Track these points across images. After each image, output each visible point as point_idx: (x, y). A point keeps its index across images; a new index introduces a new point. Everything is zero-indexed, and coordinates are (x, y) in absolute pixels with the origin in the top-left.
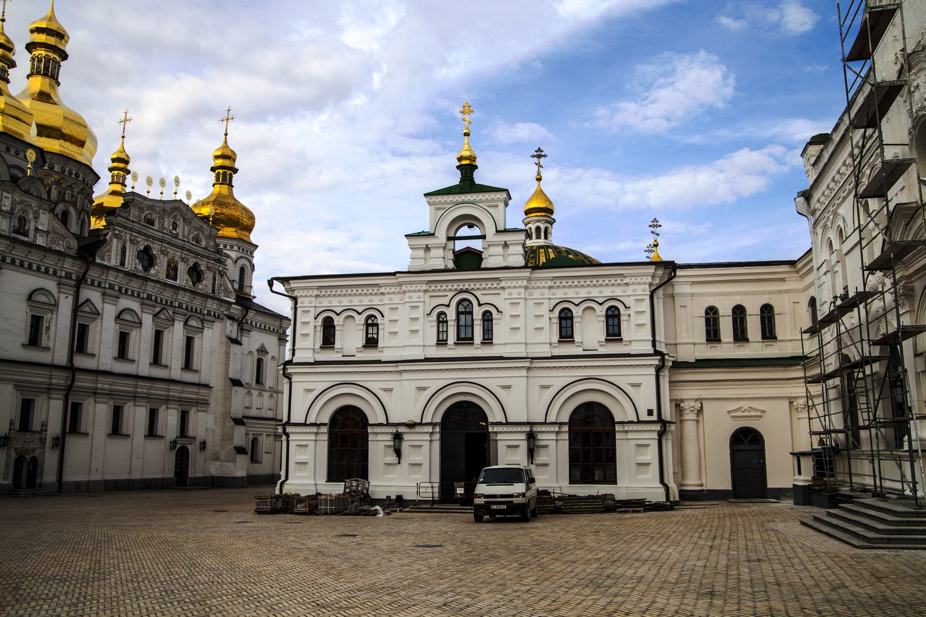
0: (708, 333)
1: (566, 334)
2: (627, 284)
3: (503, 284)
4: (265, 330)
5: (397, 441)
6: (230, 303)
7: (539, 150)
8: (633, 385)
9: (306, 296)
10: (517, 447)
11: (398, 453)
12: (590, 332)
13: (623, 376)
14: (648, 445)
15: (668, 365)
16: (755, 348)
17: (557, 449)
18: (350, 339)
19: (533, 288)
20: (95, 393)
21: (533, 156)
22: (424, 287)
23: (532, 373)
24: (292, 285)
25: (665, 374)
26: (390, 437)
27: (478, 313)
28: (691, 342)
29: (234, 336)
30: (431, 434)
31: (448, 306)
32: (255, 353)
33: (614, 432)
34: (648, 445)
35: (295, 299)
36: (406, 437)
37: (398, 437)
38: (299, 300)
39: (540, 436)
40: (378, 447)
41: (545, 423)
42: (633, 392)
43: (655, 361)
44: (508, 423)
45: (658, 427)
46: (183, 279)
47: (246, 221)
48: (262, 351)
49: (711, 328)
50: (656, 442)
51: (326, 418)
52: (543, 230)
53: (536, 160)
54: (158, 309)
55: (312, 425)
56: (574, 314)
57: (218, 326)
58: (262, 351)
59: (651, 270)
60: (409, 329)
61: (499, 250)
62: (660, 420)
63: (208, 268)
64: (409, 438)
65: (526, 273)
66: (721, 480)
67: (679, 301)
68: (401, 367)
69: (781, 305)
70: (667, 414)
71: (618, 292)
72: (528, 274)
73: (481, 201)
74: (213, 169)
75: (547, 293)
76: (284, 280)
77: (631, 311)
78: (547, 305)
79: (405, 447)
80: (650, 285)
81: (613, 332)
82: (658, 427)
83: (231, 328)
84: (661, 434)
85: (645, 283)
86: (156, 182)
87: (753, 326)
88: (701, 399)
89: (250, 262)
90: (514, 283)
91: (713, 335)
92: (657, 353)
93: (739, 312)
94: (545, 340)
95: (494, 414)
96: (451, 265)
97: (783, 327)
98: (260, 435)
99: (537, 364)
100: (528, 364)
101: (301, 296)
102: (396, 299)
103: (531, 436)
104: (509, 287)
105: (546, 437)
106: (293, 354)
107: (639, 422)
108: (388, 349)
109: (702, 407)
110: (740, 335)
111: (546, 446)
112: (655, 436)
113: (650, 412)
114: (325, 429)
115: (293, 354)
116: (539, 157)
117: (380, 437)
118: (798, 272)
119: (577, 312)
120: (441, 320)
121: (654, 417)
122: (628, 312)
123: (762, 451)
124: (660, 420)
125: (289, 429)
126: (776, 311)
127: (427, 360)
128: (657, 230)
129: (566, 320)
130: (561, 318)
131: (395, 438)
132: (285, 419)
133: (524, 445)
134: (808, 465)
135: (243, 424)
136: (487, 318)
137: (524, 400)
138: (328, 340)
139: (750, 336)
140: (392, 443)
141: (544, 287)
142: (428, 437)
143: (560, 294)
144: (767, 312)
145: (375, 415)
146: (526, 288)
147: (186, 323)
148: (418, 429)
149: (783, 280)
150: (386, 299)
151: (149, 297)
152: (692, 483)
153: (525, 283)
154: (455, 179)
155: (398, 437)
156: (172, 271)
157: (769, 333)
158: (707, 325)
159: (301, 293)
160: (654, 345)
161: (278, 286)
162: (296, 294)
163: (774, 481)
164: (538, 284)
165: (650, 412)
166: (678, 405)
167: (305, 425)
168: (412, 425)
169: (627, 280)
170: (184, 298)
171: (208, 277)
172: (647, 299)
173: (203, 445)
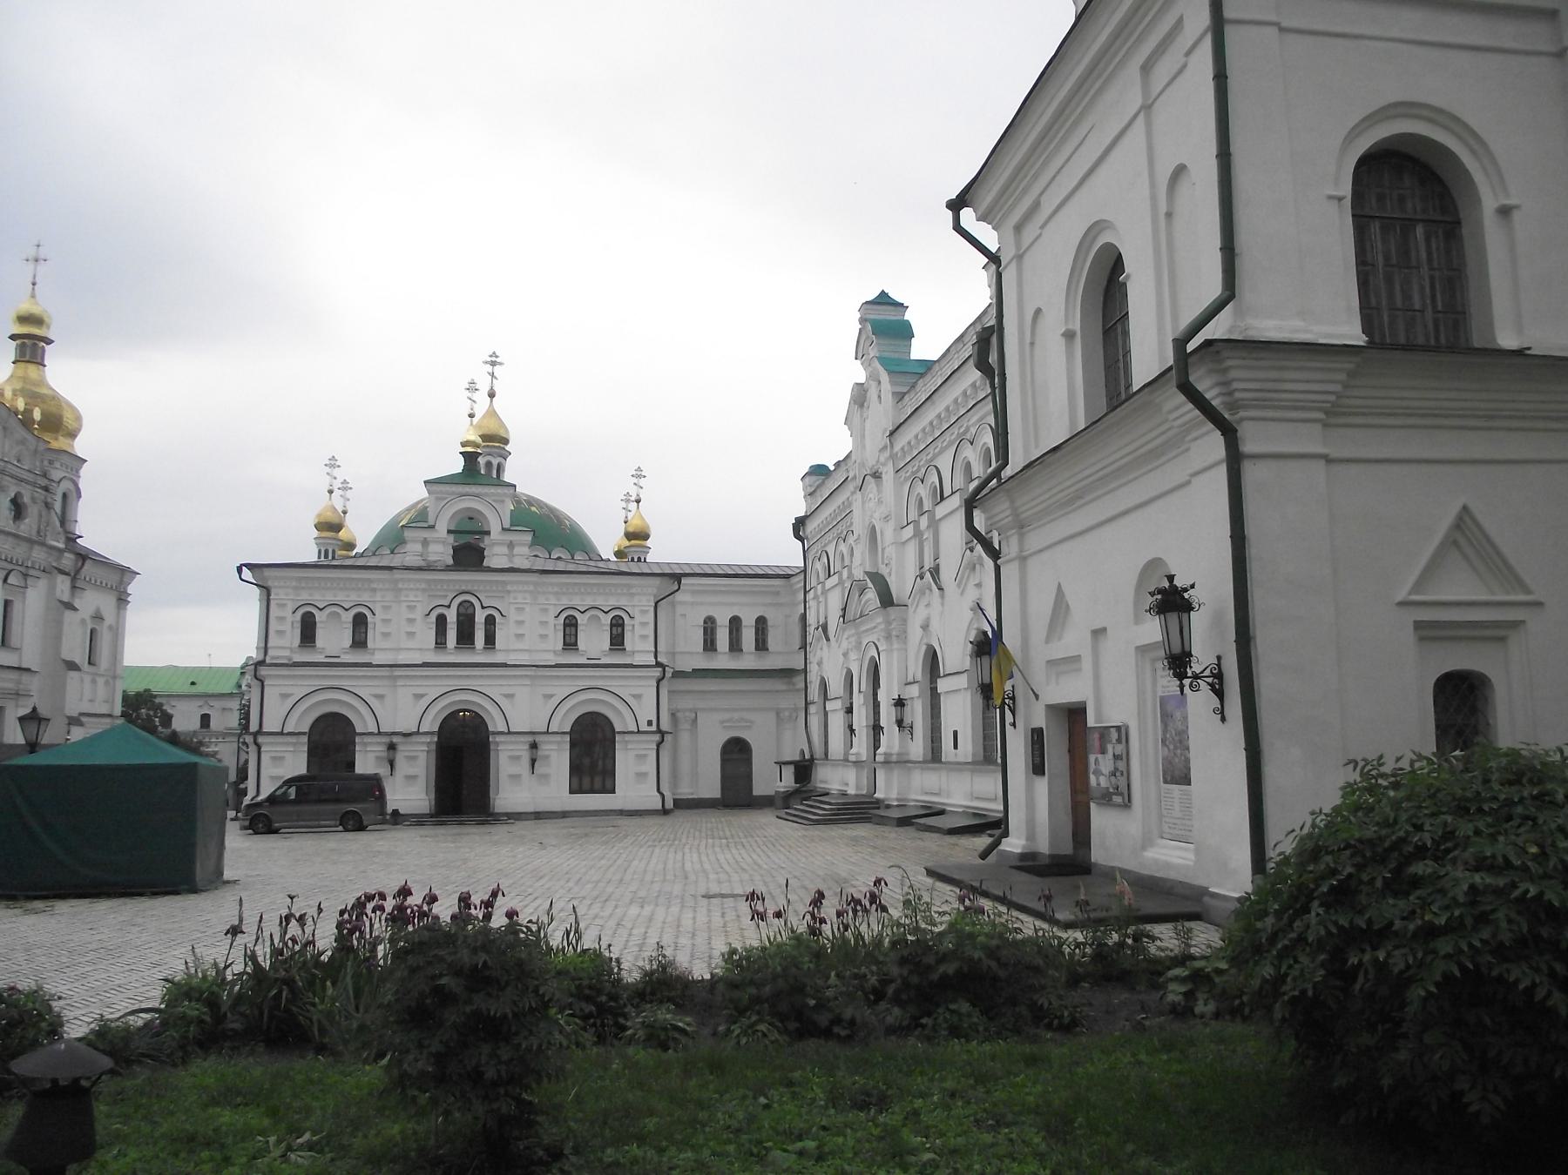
0: (705, 641)
1: (570, 644)
4: (101, 587)
12: (594, 641)
13: (626, 686)
16: (749, 661)
17: (558, 759)
18: (334, 638)
26: (383, 748)
27: (480, 617)
28: (690, 654)
29: (66, 598)
32: (89, 621)
35: (266, 590)
36: (400, 748)
37: (392, 747)
42: (633, 703)
43: (657, 672)
44: (509, 733)
45: (657, 737)
53: (489, 368)
57: (42, 584)
58: (98, 617)
59: (657, 581)
60: (404, 630)
61: (505, 550)
62: (659, 731)
63: (33, 500)
66: (710, 787)
67: (680, 610)
68: (398, 672)
69: (773, 617)
70: (665, 726)
73: (487, 495)
76: (250, 566)
77: (636, 622)
78: (553, 611)
79: (400, 758)
81: (617, 641)
82: (657, 737)
83: (63, 584)
87: (748, 637)
89: (76, 485)
91: (710, 645)
92: (658, 664)
93: (735, 623)
94: (550, 647)
95: (496, 723)
96: (451, 562)
97: (773, 641)
103: (534, 746)
108: (381, 648)
110: (735, 646)
111: (547, 757)
116: (493, 364)
120: (441, 621)
121: (654, 728)
123: (749, 762)
124: (659, 731)
125: (260, 739)
126: (770, 623)
127: (425, 665)
128: (642, 482)
129: (571, 625)
130: (565, 625)
134: (788, 773)
135: (81, 724)
136: (490, 621)
144: (761, 623)
145: (362, 722)
147: (5, 581)
152: (686, 792)
154: (458, 465)
155: (392, 747)
157: (761, 645)
161: (247, 574)
162: (270, 584)
163: (759, 789)
165: (650, 723)
167: (282, 733)
171: (33, 511)
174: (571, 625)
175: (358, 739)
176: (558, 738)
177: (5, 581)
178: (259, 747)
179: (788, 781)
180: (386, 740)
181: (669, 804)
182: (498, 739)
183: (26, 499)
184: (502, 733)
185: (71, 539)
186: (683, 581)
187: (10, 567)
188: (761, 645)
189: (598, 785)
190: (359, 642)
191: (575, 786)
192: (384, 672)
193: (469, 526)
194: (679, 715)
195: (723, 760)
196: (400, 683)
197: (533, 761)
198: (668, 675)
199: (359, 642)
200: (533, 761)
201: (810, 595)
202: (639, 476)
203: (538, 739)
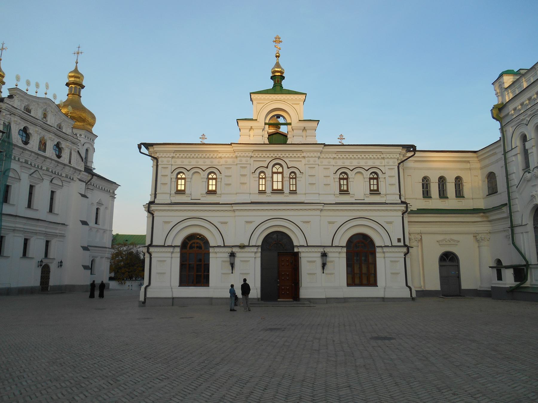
2: (383, 158)
3: (304, 154)
5: (232, 257)
6: (80, 171)
8: (387, 223)
9: (165, 157)
10: (314, 262)
11: (232, 265)
12: (359, 187)
14: (397, 261)
16: (452, 203)
19: (323, 158)
22: (251, 154)
23: (324, 213)
24: (155, 149)
25: (406, 215)
26: (227, 255)
30: (256, 253)
31: (267, 167)
32: (95, 204)
34: (397, 261)
35: (155, 159)
36: (238, 255)
37: (232, 255)
38: (160, 160)
39: (329, 255)
40: (217, 263)
41: (332, 246)
43: (403, 207)
45: (405, 250)
46: (50, 152)
47: (90, 120)
48: (100, 203)
51: (178, 242)
54: (32, 171)
55: (168, 246)
56: (350, 176)
58: (100, 203)
59: (400, 150)
62: (405, 245)
64: (240, 255)
68: (235, 207)
70: (407, 243)
71: (377, 163)
72: (321, 149)
74: (67, 85)
75: (333, 162)
76: (148, 146)
77: (386, 176)
79: (237, 261)
82: (405, 250)
85: (394, 158)
86: (33, 85)
87: (451, 189)
88: (421, 233)
89: (92, 146)
90: (312, 154)
91: (426, 194)
92: (403, 203)
93: (442, 180)
95: (297, 240)
96: (267, 142)
98: (97, 257)
99: (327, 207)
100: (321, 207)
101: (162, 157)
104: (308, 157)
106: (155, 197)
107: (392, 246)
109: (421, 239)
110: (443, 195)
111: (332, 262)
112: (402, 255)
114: (178, 250)
115: (155, 197)
117: (218, 255)
118: (477, 157)
119: (351, 174)
121: (402, 244)
122: (384, 176)
123: (458, 266)
125: (151, 249)
131: (230, 256)
132: (148, 242)
133: (319, 262)
135: (88, 250)
137: (318, 233)
139: (449, 196)
140: (228, 259)
141: (330, 158)
143: (340, 163)
144: (458, 180)
145: (213, 240)
146: (319, 158)
147: (51, 181)
148: (247, 249)
149: (468, 162)
151: (26, 162)
153: (319, 154)
155: (232, 255)
156: (43, 145)
157: (459, 194)
158: (423, 188)
159: (161, 154)
160: (400, 198)
161: (143, 149)
164: (327, 156)
165: (399, 240)
167: (164, 246)
168: (242, 247)
169: (384, 156)
173: (61, 264)
174: (344, 177)
175: (211, 250)
176: (339, 249)
177: (51, 181)
178: (150, 254)
179: (509, 279)
180: (229, 250)
181: (414, 295)
182: (300, 250)
184: (303, 246)
185: (89, 170)
188: (459, 194)
189: (365, 282)
195: (441, 266)
196: (237, 213)
197: (324, 265)
198: (409, 210)
200: (324, 265)
201: (509, 155)
202: (342, 139)
203: (327, 250)
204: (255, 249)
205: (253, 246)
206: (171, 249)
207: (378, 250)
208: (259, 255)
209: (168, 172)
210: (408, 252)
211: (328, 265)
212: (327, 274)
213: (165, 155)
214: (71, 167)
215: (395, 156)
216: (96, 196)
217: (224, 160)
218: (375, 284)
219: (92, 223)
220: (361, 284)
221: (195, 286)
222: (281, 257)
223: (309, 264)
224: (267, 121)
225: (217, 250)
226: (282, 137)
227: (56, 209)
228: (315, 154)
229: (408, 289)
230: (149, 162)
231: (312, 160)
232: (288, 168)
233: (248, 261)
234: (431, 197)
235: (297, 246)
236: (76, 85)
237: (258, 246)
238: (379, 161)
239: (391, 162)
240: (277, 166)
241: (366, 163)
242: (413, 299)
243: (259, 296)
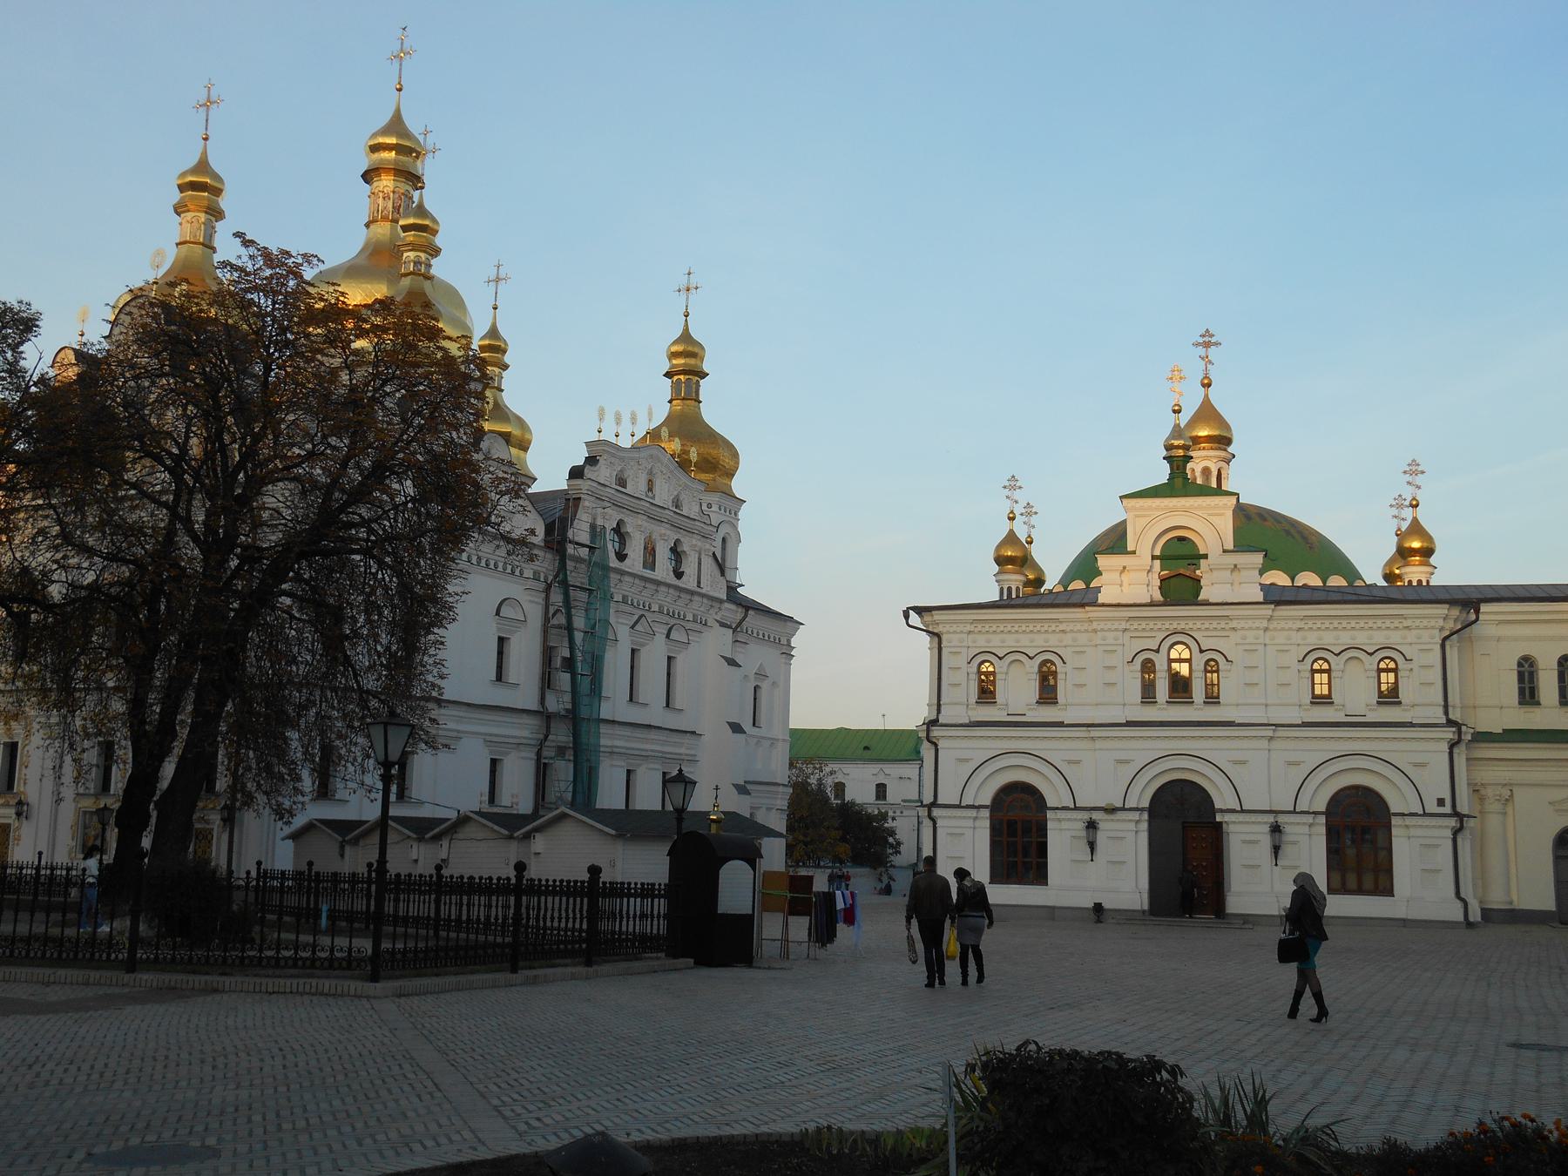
0: (1522, 692)
3: (1234, 624)
4: (765, 640)
6: (721, 601)
7: (1207, 333)
10: (1256, 842)
11: (1092, 846)
14: (1437, 846)
15: (1463, 738)
20: (612, 753)
21: (1197, 345)
22: (1124, 625)
23: (1276, 744)
26: (1081, 825)
28: (1496, 704)
30: (1137, 822)
31: (1157, 651)
32: (752, 676)
33: (1389, 827)
34: (1437, 846)
35: (937, 636)
36: (1101, 825)
37: (1092, 826)
38: (944, 637)
39: (1287, 829)
40: (1061, 838)
41: (1294, 812)
43: (1450, 733)
46: (664, 569)
47: (726, 461)
48: (761, 675)
49: (1527, 685)
50: (1450, 843)
51: (986, 799)
52: (1215, 473)
53: (1201, 351)
55: (968, 807)
58: (761, 675)
59: (1442, 610)
62: (1456, 814)
64: (1107, 825)
65: (1267, 610)
68: (1096, 732)
70: (1463, 808)
73: (1200, 507)
74: (668, 375)
75: (1297, 637)
76: (920, 611)
79: (1101, 838)
80: (1442, 629)
82: (1453, 822)
84: (1456, 832)
86: (626, 419)
89: (735, 527)
90: (1250, 623)
91: (1528, 694)
92: (1450, 723)
95: (1222, 798)
96: (1158, 596)
99: (1282, 732)
102: (1083, 638)
103: (1276, 829)
105: (1295, 829)
106: (939, 711)
107: (1425, 814)
111: (1294, 843)
112: (1449, 834)
113: (1441, 802)
114: (986, 813)
115: (939, 711)
116: (1207, 345)
117: (1065, 825)
121: (1447, 809)
125: (936, 812)
127: (1129, 724)
128: (1419, 480)
132: (928, 799)
133: (1266, 841)
135: (747, 793)
138: (986, 693)
140: (1084, 833)
142: (1132, 826)
143: (1313, 639)
146: (1266, 629)
147: (668, 636)
148: (1120, 815)
150: (1068, 639)
152: (1497, 900)
153: (1265, 623)
155: (1092, 826)
160: (1446, 713)
164: (1282, 624)
165: (1441, 802)
166: (1476, 790)
167: (959, 806)
168: (1111, 810)
169: (1408, 623)
170: (665, 598)
172: (1438, 648)
175: (1049, 814)
177: (668, 636)
180: (1086, 816)
181: (1475, 915)
182: (1227, 818)
183: (685, 547)
184: (1233, 811)
185: (732, 589)
186: (1484, 608)
187: (673, 621)
190: (1048, 693)
191: (1337, 883)
192: (1081, 732)
193: (1183, 549)
194: (1489, 792)
195: (1558, 859)
196: (1099, 744)
199: (1048, 693)
200: (1276, 849)
202: (1416, 473)
203: (1282, 819)
204: (1135, 816)
205: (1131, 809)
206: (973, 813)
207: (1395, 821)
208: (1145, 826)
209: (961, 661)
210: (1461, 828)
211: (1287, 850)
212: (1284, 868)
213: (955, 627)
214: (703, 596)
215: (1433, 623)
216: (755, 656)
217: (1069, 636)
218: (1388, 891)
219: (747, 726)
220: (1360, 891)
221: (1020, 882)
222: (1186, 830)
223: (1244, 848)
224: (1157, 553)
225: (1060, 814)
226: (1190, 582)
227: (678, 702)
228: (1257, 624)
229: (1459, 905)
230: (926, 638)
231: (1250, 635)
232: (1201, 651)
233: (1122, 838)
234: (1538, 703)
235: (1222, 811)
236: (687, 369)
237: (1142, 810)
238: (1400, 633)
239: (1425, 635)
240: (1180, 647)
241: (1370, 638)
242: (1470, 925)
243: (1146, 907)
